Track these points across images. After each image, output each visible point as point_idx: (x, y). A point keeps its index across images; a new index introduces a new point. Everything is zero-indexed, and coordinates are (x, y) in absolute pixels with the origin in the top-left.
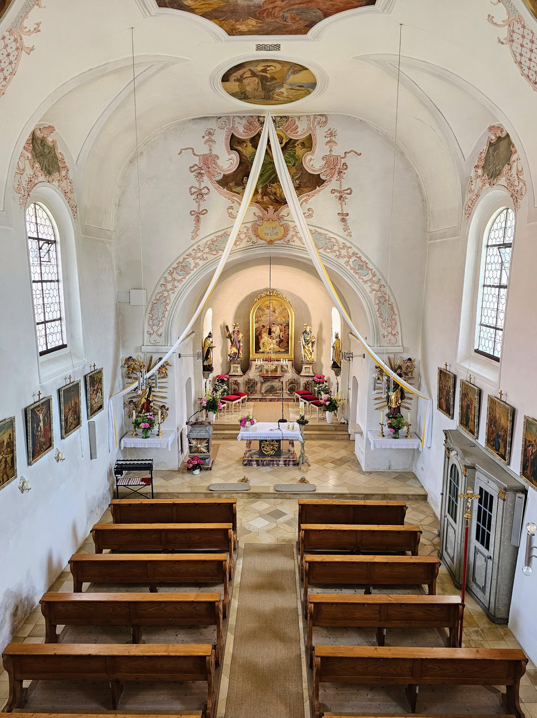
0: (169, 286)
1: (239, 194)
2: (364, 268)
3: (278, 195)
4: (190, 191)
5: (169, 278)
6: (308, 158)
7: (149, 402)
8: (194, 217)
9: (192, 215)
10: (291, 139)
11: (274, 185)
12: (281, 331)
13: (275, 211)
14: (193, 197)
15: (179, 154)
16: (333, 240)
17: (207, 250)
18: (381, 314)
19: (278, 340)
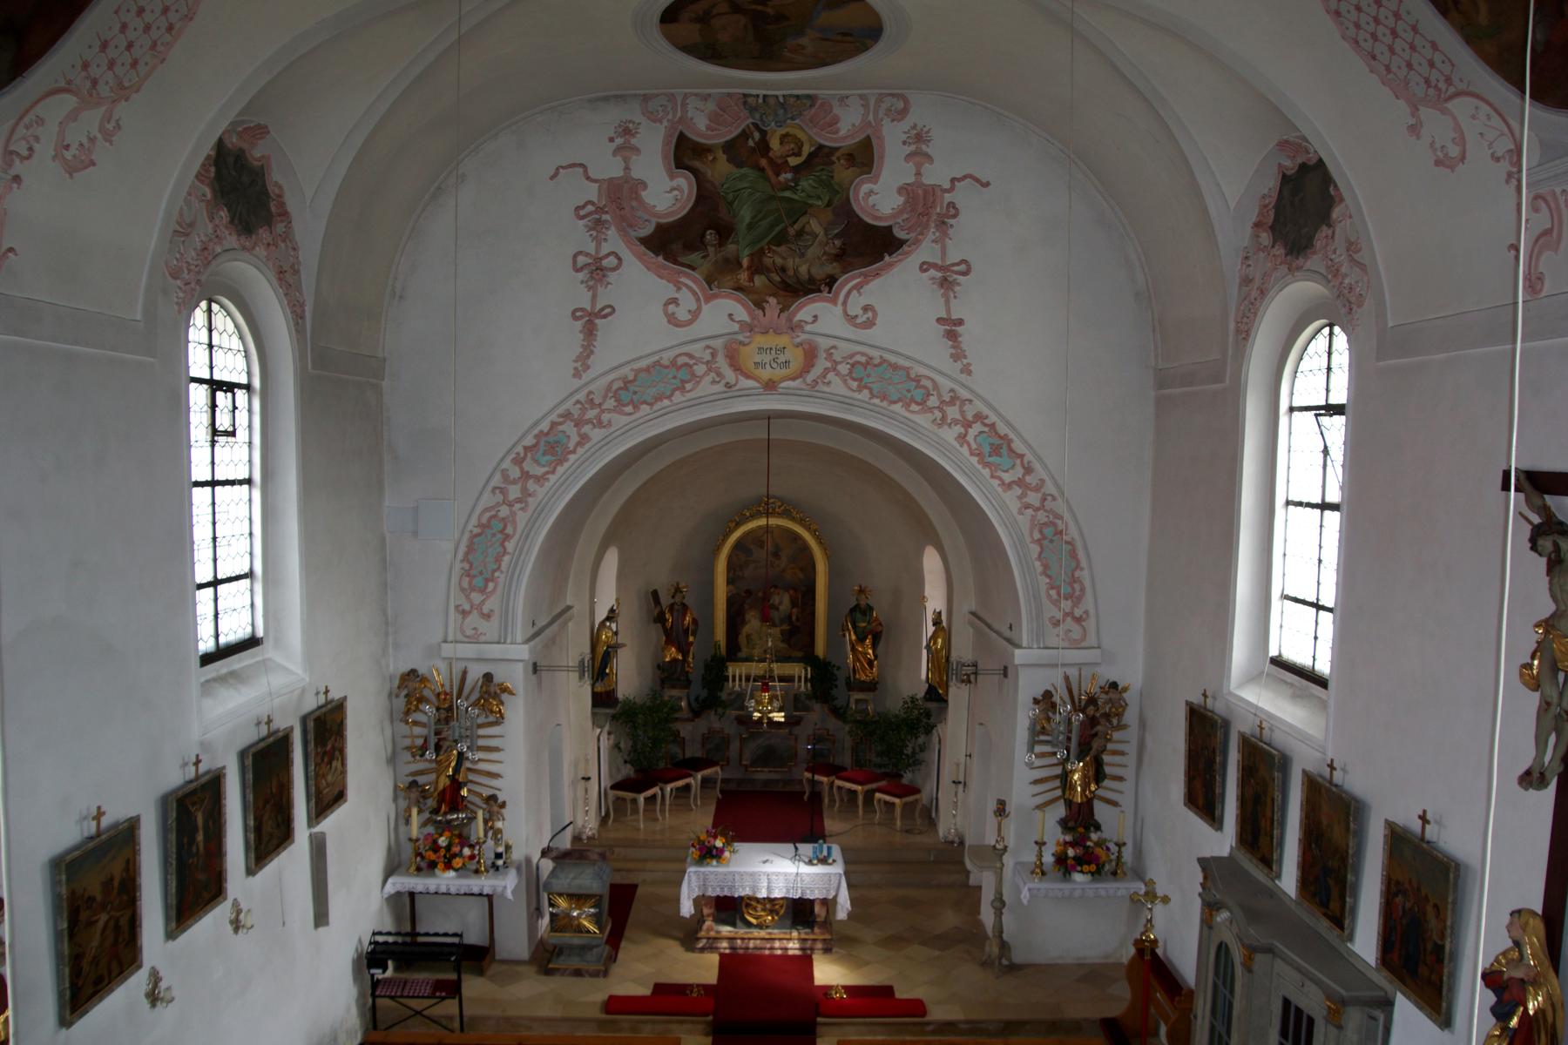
0: (514, 492)
1: (693, 269)
2: (1004, 451)
3: (791, 273)
4: (575, 262)
6: (865, 188)
7: (456, 784)
8: (579, 324)
9: (576, 318)
10: (821, 147)
11: (779, 249)
12: (794, 604)
13: (782, 311)
14: (581, 276)
15: (552, 178)
16: (924, 382)
17: (610, 403)
18: (1046, 567)
19: (785, 627)
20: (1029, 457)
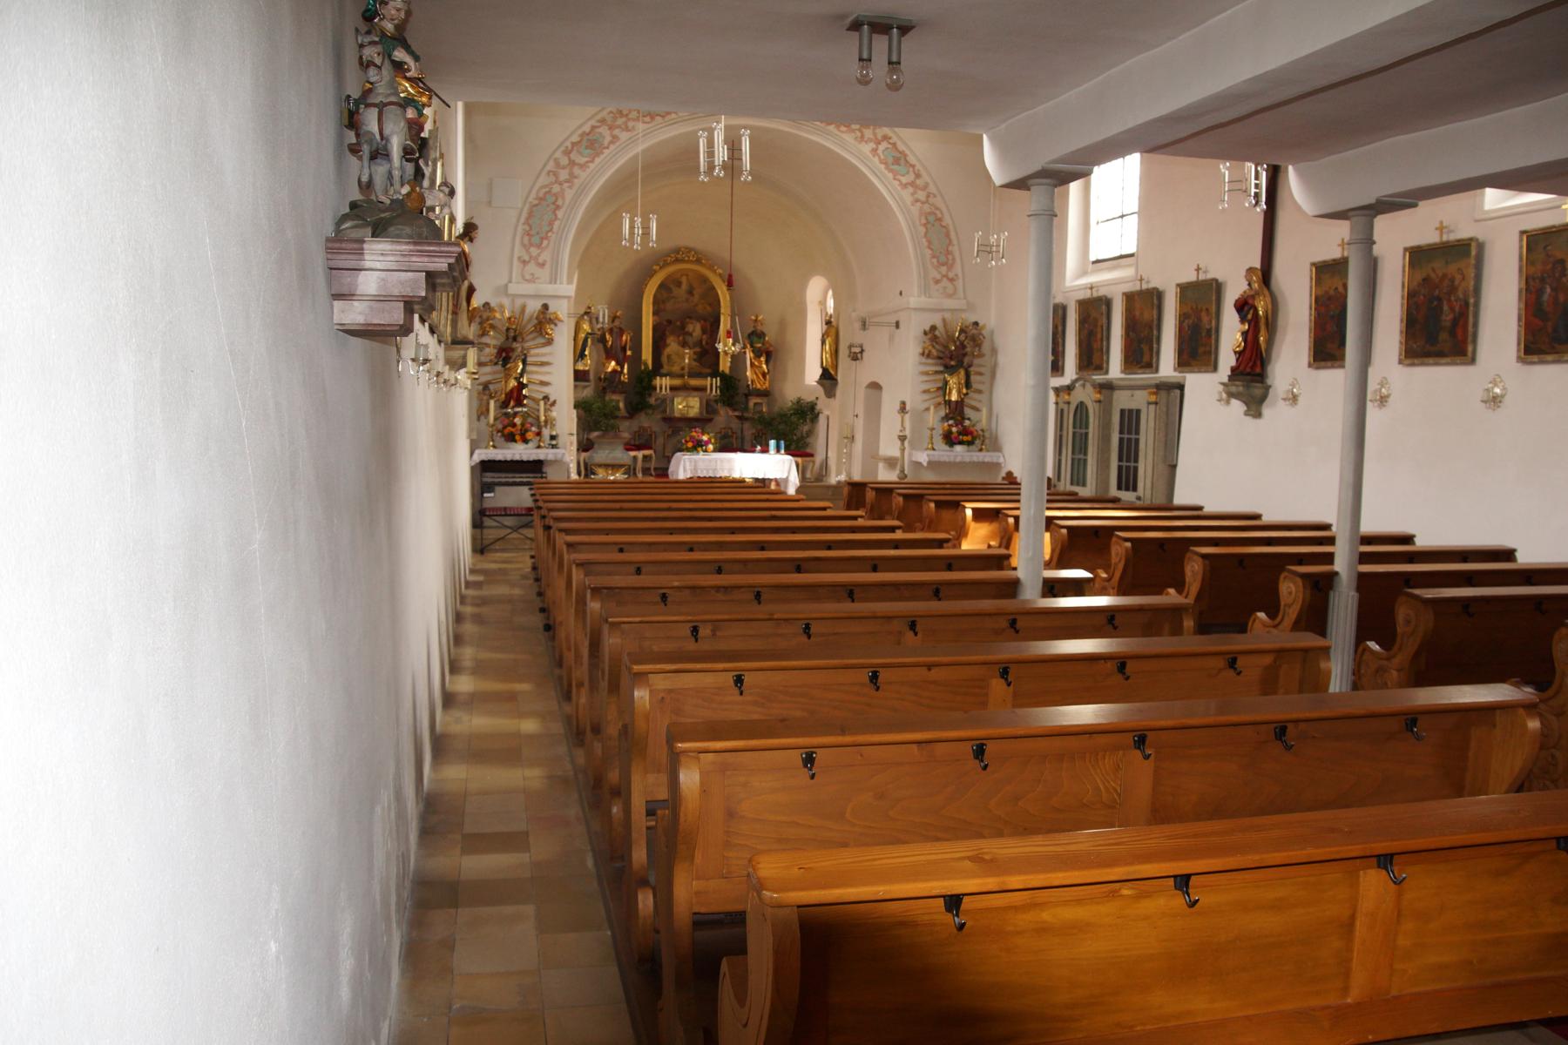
0: (564, 175)
5: (564, 161)
12: (704, 331)
18: (929, 242)
20: (918, 166)
